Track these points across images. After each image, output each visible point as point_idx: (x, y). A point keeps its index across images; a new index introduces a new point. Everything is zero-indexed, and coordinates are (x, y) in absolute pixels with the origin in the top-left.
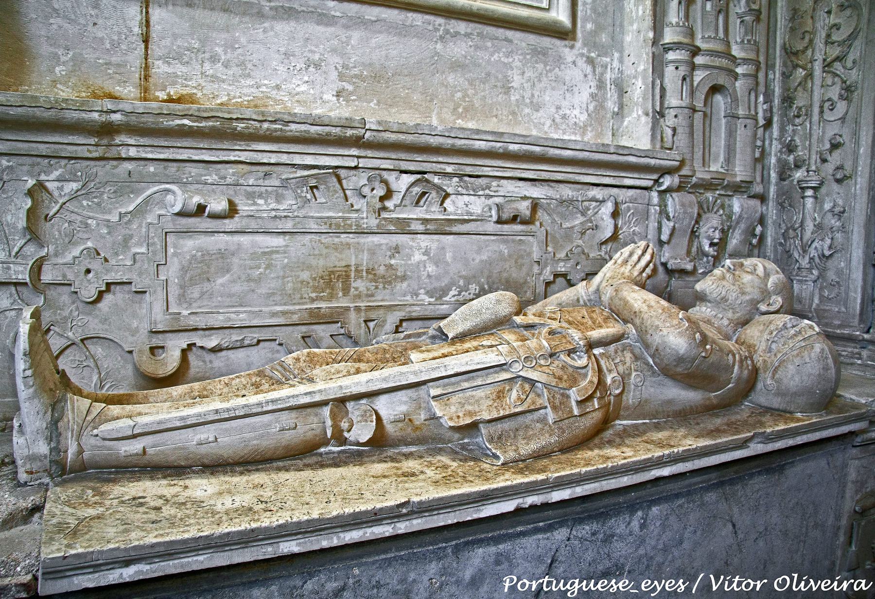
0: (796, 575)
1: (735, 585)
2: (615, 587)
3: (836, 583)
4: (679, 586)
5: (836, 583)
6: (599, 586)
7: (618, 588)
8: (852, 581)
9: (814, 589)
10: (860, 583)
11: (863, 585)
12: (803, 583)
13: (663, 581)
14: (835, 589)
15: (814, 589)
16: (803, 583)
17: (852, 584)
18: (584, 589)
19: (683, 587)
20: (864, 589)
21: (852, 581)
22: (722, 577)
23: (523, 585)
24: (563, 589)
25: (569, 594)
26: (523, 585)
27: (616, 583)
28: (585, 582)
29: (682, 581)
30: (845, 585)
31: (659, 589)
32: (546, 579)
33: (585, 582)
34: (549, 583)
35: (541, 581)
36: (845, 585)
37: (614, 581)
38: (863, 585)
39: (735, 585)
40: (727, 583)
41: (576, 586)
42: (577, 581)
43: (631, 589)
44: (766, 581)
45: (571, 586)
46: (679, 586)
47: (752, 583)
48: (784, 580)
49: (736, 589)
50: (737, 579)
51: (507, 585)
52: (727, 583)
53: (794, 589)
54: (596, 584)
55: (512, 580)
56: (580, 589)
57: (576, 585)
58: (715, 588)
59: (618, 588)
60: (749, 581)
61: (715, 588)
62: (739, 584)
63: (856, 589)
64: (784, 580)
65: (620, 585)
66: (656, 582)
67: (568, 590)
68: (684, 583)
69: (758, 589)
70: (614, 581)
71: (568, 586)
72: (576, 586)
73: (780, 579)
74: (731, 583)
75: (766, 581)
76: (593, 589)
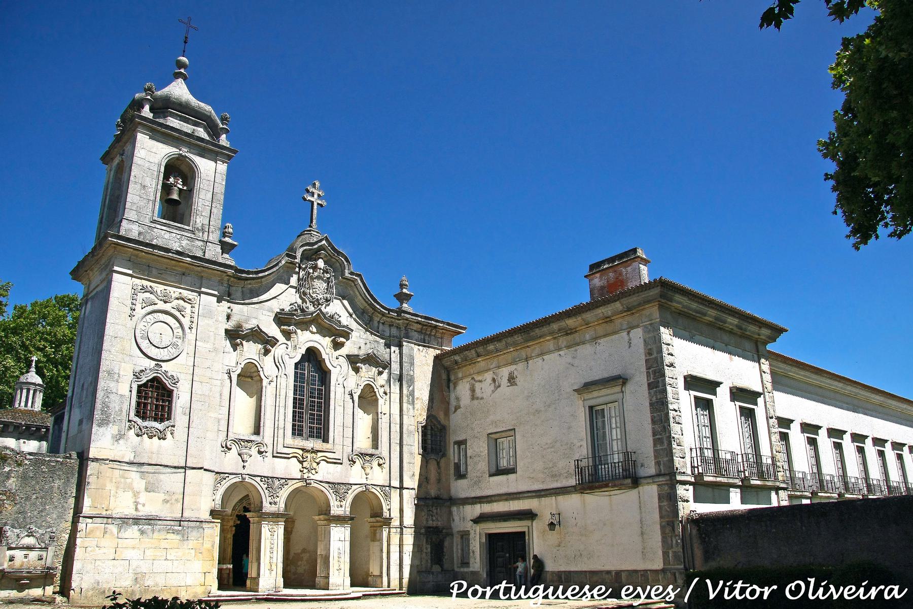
0: (812, 580)
1: (737, 592)
3: (862, 590)
4: (668, 594)
5: (862, 590)
8: (882, 587)
9: (835, 597)
10: (891, 590)
11: (895, 592)
12: (821, 590)
13: (649, 587)
14: (862, 597)
15: (835, 597)
16: (821, 590)
19: (672, 595)
20: (897, 597)
21: (882, 587)
27: (590, 590)
28: (552, 588)
29: (671, 587)
30: (873, 592)
32: (504, 584)
33: (552, 588)
35: (497, 587)
36: (873, 592)
38: (895, 592)
39: (737, 592)
40: (727, 589)
42: (542, 587)
44: (775, 587)
45: (534, 593)
46: (668, 594)
47: (758, 590)
48: (798, 587)
50: (740, 585)
52: (727, 589)
53: (811, 597)
57: (540, 592)
58: (712, 596)
60: (755, 587)
61: (712, 596)
62: (743, 591)
63: (887, 597)
64: (798, 587)
65: (595, 592)
66: (639, 589)
68: (673, 590)
69: (765, 597)
70: (587, 587)
73: (793, 585)
74: (732, 589)
75: (775, 587)
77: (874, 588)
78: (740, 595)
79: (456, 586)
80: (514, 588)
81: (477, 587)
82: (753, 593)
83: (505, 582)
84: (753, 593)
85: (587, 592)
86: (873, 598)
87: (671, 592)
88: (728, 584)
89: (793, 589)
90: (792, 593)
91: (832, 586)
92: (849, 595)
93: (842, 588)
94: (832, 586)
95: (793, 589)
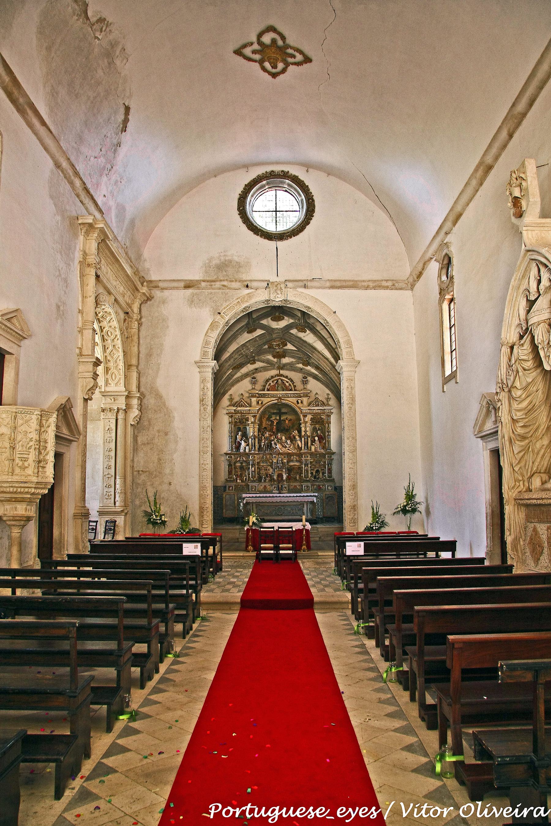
1: (423, 812)
2: (313, 814)
4: (372, 813)
6: (298, 813)
7: (315, 814)
8: (532, 808)
9: (497, 815)
10: (539, 811)
11: (542, 812)
12: (486, 811)
13: (357, 808)
14: (517, 816)
15: (497, 815)
16: (486, 811)
17: (532, 812)
18: (284, 816)
19: (375, 814)
20: (543, 815)
21: (532, 808)
22: (412, 805)
23: (228, 812)
24: (264, 816)
25: (270, 821)
26: (228, 812)
27: (314, 810)
28: (285, 809)
30: (525, 812)
31: (353, 816)
32: (249, 806)
33: (285, 809)
34: (252, 811)
35: (244, 808)
36: (525, 812)
37: (312, 808)
38: (542, 812)
39: (423, 812)
40: (416, 810)
41: (277, 813)
42: (277, 808)
43: (327, 815)
45: (272, 813)
46: (372, 813)
48: (469, 808)
49: (424, 816)
50: (425, 807)
51: (213, 812)
52: (416, 810)
54: (294, 812)
55: (217, 807)
56: (280, 816)
57: (276, 812)
58: (405, 815)
59: (315, 814)
61: (405, 815)
62: (427, 811)
63: (535, 816)
64: (469, 808)
65: (317, 812)
66: (350, 810)
67: (268, 817)
68: (376, 811)
70: (312, 808)
71: (269, 813)
72: (277, 813)
73: (465, 806)
76: (292, 816)
77: (526, 809)
78: (426, 814)
79: (214, 808)
80: (257, 809)
81: (229, 808)
82: (435, 812)
83: (250, 804)
84: (435, 812)
85: (311, 812)
86: (525, 816)
87: (374, 812)
88: (417, 806)
89: (465, 809)
90: (464, 812)
91: (494, 808)
92: (507, 814)
93: (502, 809)
94: (494, 808)
95: (465, 809)
